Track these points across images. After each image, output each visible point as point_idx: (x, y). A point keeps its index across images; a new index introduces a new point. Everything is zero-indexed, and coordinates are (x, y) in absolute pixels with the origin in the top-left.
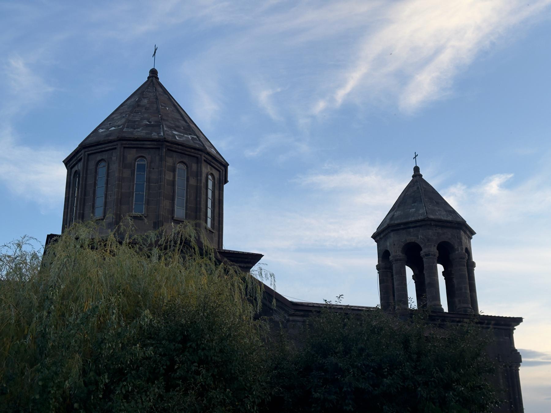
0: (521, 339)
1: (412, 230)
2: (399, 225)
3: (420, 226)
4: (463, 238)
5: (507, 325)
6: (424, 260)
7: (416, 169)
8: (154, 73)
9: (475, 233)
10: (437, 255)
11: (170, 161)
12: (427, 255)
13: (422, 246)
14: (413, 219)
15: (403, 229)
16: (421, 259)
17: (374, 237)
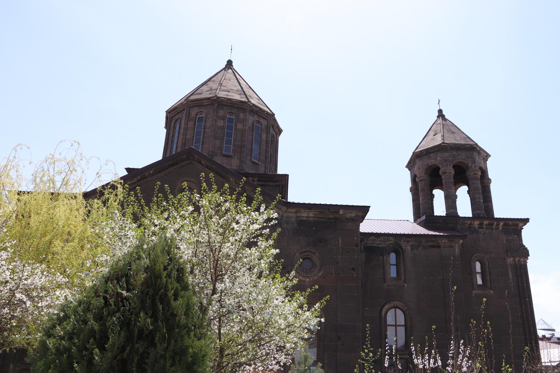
0: (528, 236)
1: (432, 155)
3: (438, 151)
4: (477, 158)
5: (515, 226)
6: (443, 177)
7: (440, 111)
9: (490, 156)
10: (453, 173)
11: (221, 113)
12: (444, 173)
13: (440, 166)
14: (432, 146)
15: (426, 155)
16: (440, 177)
17: (407, 167)
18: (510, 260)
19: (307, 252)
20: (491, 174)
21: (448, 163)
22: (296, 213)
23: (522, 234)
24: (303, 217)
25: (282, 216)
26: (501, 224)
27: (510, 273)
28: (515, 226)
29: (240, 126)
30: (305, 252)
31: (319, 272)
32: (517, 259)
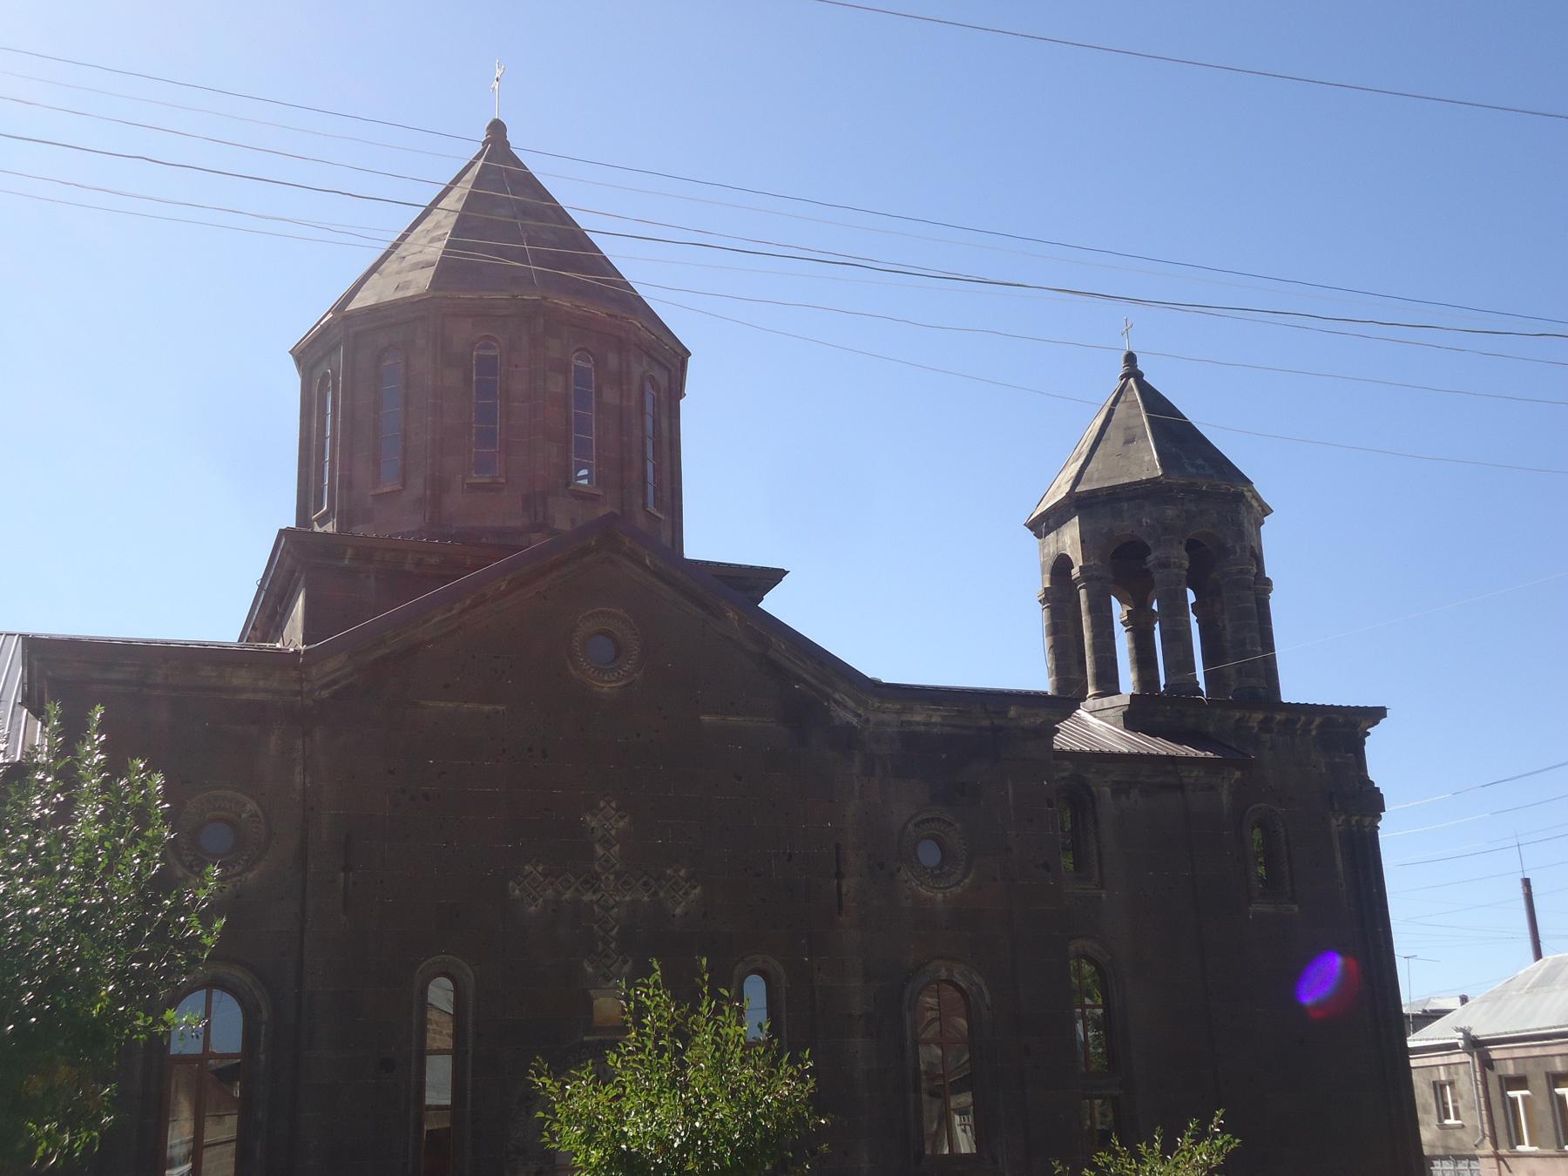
0: (1382, 757)
1: (1125, 505)
2: (1092, 494)
5: (1347, 728)
7: (1130, 358)
8: (497, 128)
10: (1186, 564)
12: (1165, 565)
13: (1150, 543)
14: (1127, 480)
18: (1337, 823)
19: (933, 820)
20: (1272, 568)
21: (1166, 535)
22: (899, 713)
23: (1366, 748)
24: (918, 723)
25: (867, 720)
26: (1318, 721)
27: (1339, 857)
28: (1347, 728)
29: (611, 396)
30: (928, 820)
31: (965, 876)
32: (1354, 820)
